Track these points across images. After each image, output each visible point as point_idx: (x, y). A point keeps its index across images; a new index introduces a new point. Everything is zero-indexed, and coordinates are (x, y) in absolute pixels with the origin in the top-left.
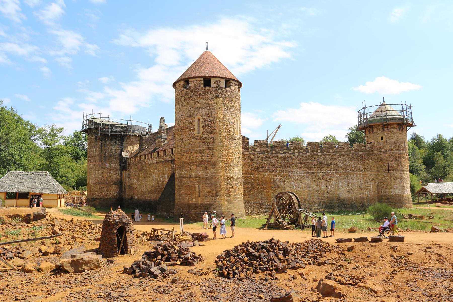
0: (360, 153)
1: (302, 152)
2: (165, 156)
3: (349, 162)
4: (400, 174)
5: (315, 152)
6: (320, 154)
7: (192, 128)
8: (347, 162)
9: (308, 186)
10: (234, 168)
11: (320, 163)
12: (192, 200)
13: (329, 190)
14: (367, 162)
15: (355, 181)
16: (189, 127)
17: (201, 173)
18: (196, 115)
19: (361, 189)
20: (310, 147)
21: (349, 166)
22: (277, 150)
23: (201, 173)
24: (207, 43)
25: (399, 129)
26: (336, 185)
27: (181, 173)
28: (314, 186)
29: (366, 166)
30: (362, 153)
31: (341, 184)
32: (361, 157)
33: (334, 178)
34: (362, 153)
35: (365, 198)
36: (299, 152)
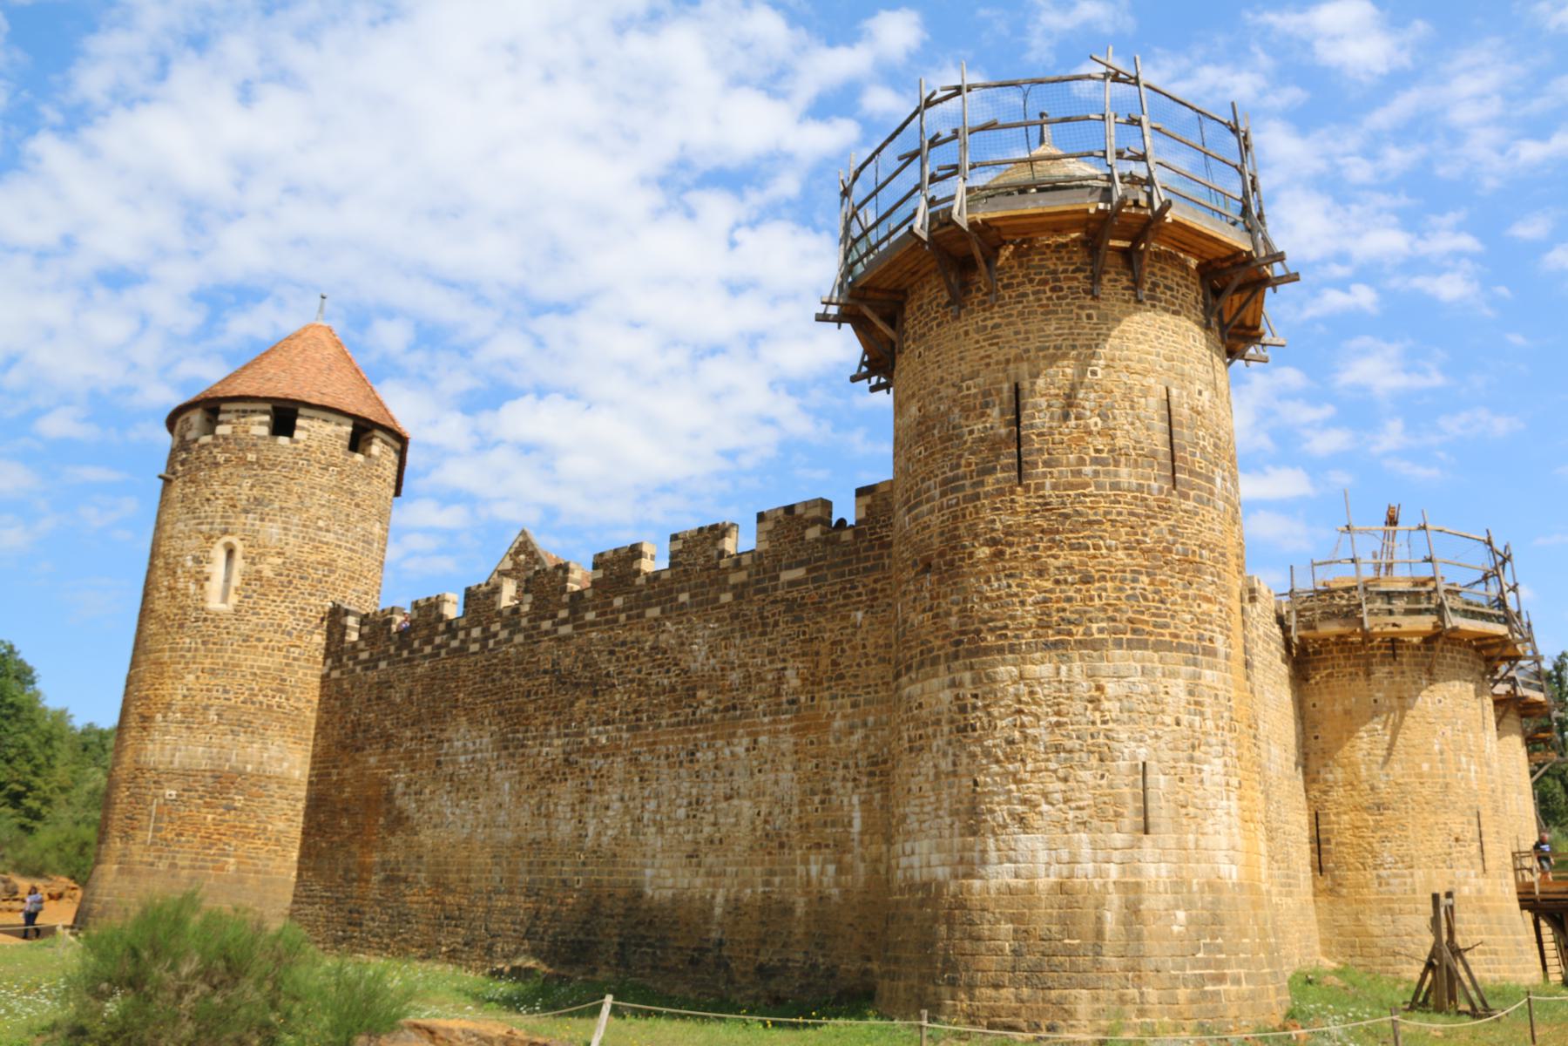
0: (786, 576)
1: (495, 635)
3: (712, 650)
4: (947, 695)
5: (546, 625)
6: (565, 630)
8: (699, 657)
9: (502, 817)
10: (167, 733)
11: (562, 679)
13: (589, 843)
14: (830, 629)
15: (741, 781)
19: (773, 842)
20: (529, 598)
21: (707, 681)
22: (416, 644)
25: (959, 299)
26: (627, 810)
28: (525, 817)
29: (825, 662)
30: (799, 573)
31: (652, 805)
32: (791, 605)
33: (619, 765)
34: (799, 573)
35: (800, 910)
36: (487, 635)
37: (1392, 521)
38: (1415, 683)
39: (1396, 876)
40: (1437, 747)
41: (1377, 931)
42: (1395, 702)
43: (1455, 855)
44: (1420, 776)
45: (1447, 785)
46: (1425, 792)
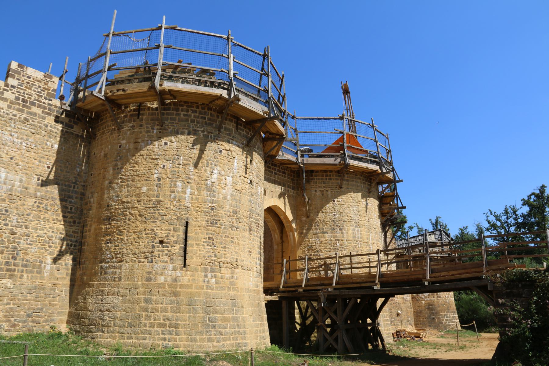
37: (346, 92)
38: (148, 132)
39: (111, 267)
40: (156, 176)
41: (90, 307)
42: (132, 146)
43: (156, 253)
44: (138, 196)
45: (159, 202)
46: (140, 207)
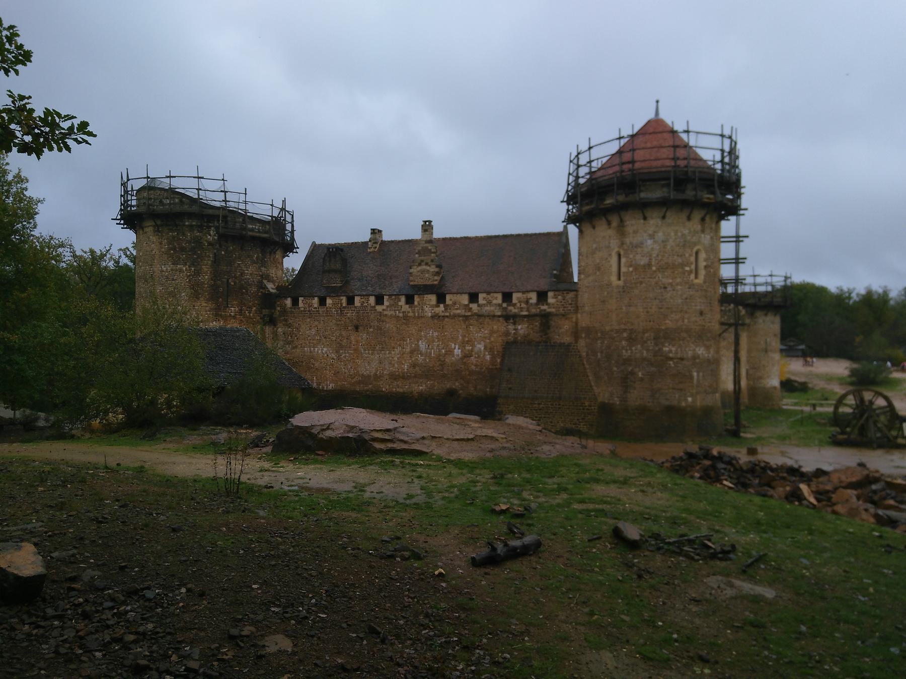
2: (474, 306)
7: (687, 269)
12: (686, 400)
16: (683, 265)
17: (701, 351)
18: (695, 244)
23: (701, 351)
24: (657, 102)
27: (661, 350)
